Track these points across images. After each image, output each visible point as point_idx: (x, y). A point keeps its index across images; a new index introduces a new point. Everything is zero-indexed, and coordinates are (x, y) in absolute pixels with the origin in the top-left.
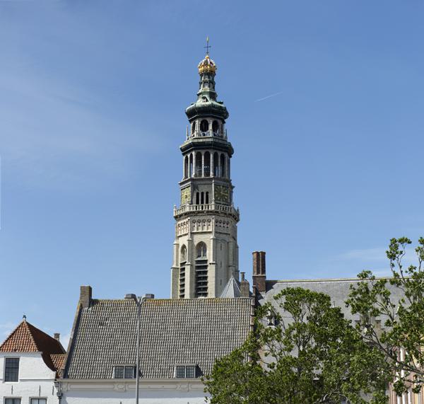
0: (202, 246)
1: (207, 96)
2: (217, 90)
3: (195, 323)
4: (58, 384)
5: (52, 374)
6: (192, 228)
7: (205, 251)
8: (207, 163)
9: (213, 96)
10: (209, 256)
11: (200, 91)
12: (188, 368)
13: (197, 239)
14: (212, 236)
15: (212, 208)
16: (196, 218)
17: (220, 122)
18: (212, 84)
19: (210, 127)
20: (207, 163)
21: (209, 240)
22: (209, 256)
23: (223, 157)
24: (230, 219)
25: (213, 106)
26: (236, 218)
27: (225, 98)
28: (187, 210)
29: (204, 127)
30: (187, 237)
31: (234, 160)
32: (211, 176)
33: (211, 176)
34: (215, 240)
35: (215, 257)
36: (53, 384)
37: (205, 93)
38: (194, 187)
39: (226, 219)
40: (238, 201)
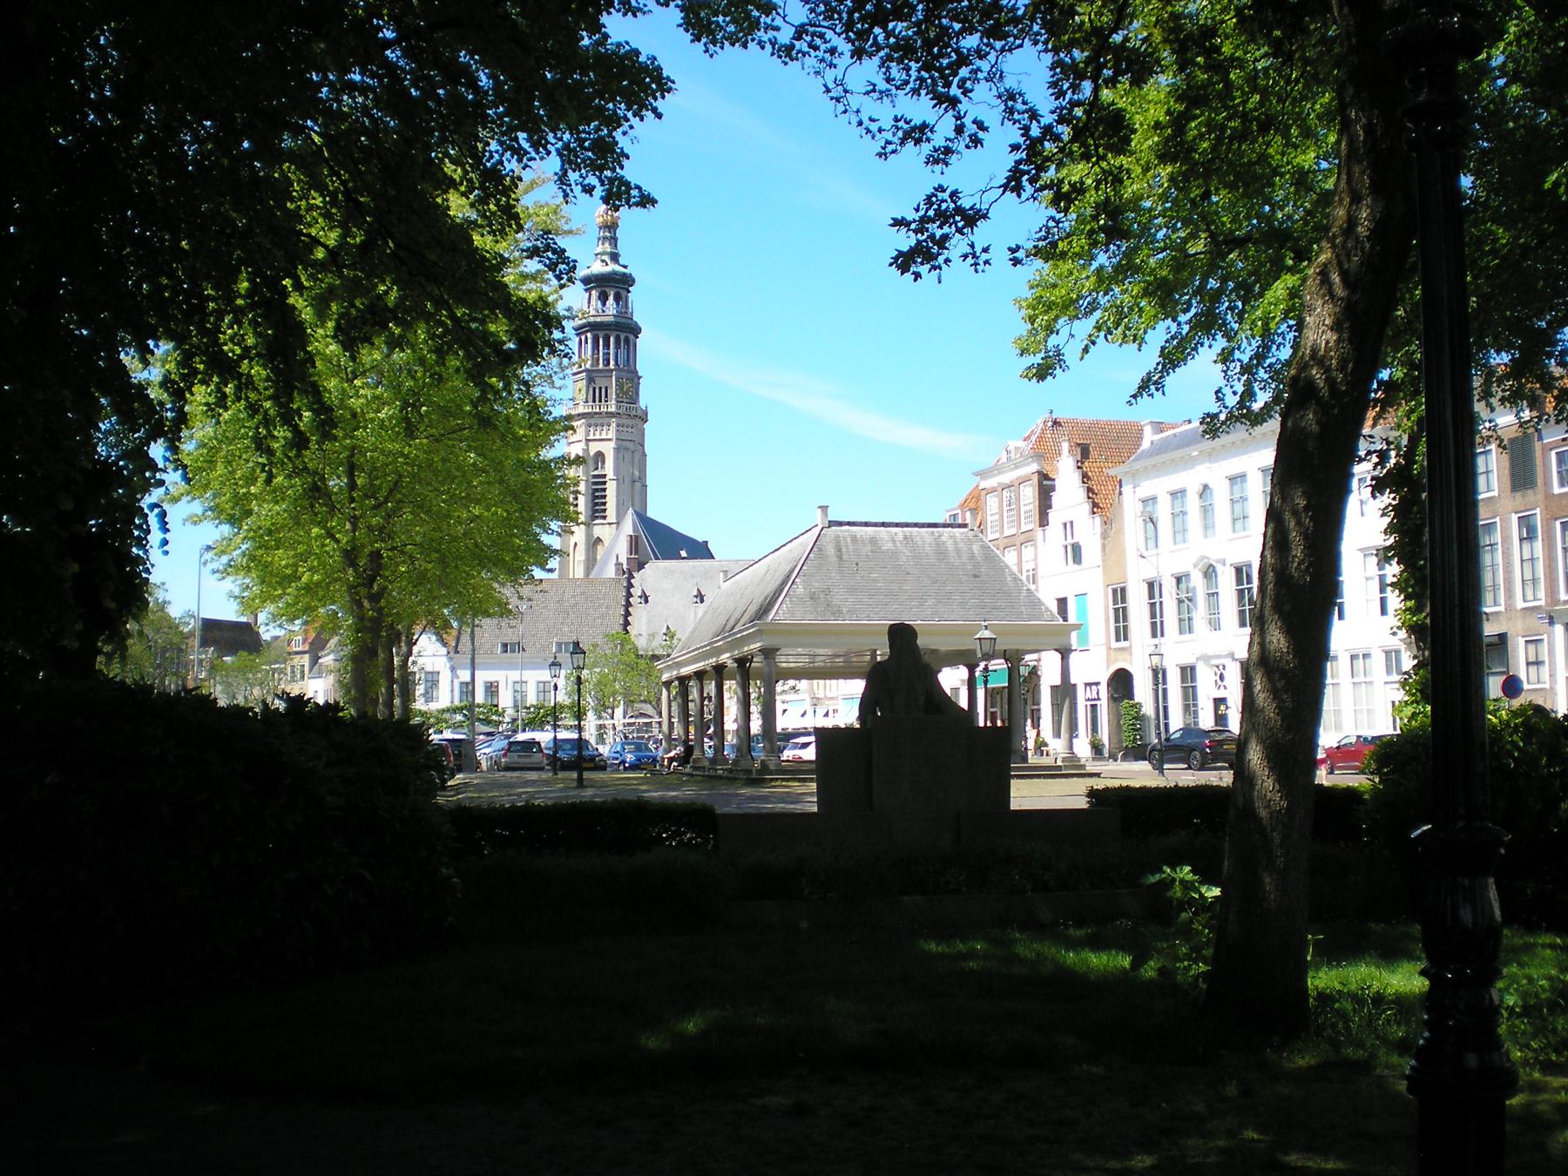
0: (600, 456)
1: (606, 258)
2: (621, 248)
3: (572, 602)
4: (450, 659)
5: (444, 651)
6: (588, 433)
7: (603, 462)
8: (607, 345)
9: (615, 257)
10: (609, 469)
11: (599, 249)
12: (567, 644)
13: (594, 448)
14: (612, 444)
15: (613, 409)
16: (593, 421)
17: (623, 293)
18: (614, 240)
19: (611, 298)
20: (607, 345)
21: (608, 449)
22: (609, 469)
23: (627, 341)
24: (638, 421)
25: (615, 273)
26: (643, 418)
27: (632, 262)
28: (581, 410)
29: (603, 298)
30: (582, 445)
31: (642, 342)
32: (612, 366)
33: (612, 366)
34: (617, 450)
35: (617, 472)
36: (445, 659)
37: (604, 253)
38: (591, 380)
39: (630, 422)
40: (645, 399)
